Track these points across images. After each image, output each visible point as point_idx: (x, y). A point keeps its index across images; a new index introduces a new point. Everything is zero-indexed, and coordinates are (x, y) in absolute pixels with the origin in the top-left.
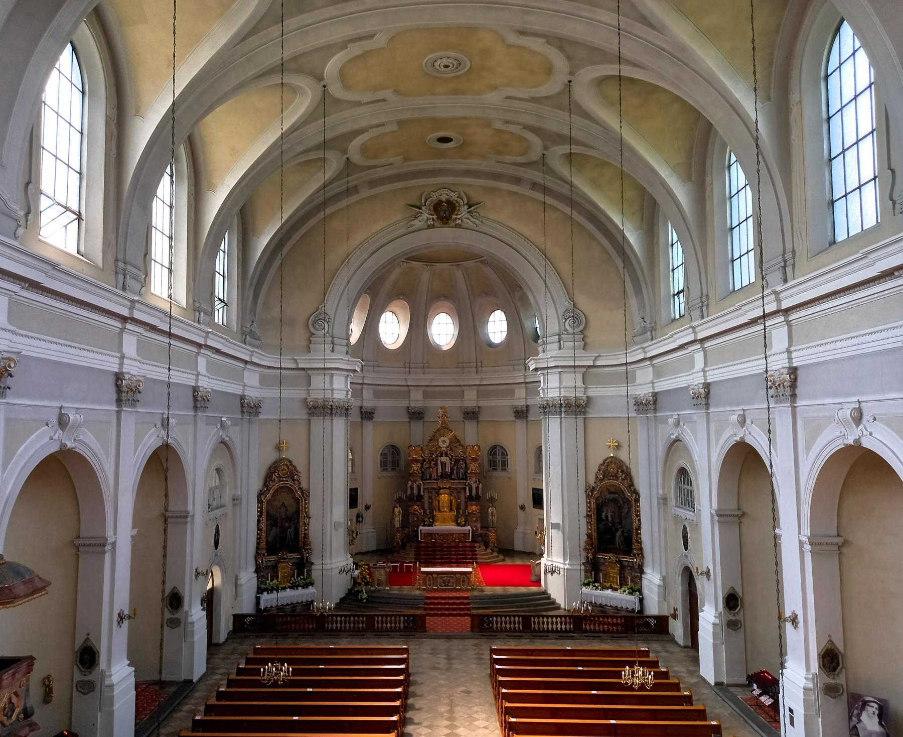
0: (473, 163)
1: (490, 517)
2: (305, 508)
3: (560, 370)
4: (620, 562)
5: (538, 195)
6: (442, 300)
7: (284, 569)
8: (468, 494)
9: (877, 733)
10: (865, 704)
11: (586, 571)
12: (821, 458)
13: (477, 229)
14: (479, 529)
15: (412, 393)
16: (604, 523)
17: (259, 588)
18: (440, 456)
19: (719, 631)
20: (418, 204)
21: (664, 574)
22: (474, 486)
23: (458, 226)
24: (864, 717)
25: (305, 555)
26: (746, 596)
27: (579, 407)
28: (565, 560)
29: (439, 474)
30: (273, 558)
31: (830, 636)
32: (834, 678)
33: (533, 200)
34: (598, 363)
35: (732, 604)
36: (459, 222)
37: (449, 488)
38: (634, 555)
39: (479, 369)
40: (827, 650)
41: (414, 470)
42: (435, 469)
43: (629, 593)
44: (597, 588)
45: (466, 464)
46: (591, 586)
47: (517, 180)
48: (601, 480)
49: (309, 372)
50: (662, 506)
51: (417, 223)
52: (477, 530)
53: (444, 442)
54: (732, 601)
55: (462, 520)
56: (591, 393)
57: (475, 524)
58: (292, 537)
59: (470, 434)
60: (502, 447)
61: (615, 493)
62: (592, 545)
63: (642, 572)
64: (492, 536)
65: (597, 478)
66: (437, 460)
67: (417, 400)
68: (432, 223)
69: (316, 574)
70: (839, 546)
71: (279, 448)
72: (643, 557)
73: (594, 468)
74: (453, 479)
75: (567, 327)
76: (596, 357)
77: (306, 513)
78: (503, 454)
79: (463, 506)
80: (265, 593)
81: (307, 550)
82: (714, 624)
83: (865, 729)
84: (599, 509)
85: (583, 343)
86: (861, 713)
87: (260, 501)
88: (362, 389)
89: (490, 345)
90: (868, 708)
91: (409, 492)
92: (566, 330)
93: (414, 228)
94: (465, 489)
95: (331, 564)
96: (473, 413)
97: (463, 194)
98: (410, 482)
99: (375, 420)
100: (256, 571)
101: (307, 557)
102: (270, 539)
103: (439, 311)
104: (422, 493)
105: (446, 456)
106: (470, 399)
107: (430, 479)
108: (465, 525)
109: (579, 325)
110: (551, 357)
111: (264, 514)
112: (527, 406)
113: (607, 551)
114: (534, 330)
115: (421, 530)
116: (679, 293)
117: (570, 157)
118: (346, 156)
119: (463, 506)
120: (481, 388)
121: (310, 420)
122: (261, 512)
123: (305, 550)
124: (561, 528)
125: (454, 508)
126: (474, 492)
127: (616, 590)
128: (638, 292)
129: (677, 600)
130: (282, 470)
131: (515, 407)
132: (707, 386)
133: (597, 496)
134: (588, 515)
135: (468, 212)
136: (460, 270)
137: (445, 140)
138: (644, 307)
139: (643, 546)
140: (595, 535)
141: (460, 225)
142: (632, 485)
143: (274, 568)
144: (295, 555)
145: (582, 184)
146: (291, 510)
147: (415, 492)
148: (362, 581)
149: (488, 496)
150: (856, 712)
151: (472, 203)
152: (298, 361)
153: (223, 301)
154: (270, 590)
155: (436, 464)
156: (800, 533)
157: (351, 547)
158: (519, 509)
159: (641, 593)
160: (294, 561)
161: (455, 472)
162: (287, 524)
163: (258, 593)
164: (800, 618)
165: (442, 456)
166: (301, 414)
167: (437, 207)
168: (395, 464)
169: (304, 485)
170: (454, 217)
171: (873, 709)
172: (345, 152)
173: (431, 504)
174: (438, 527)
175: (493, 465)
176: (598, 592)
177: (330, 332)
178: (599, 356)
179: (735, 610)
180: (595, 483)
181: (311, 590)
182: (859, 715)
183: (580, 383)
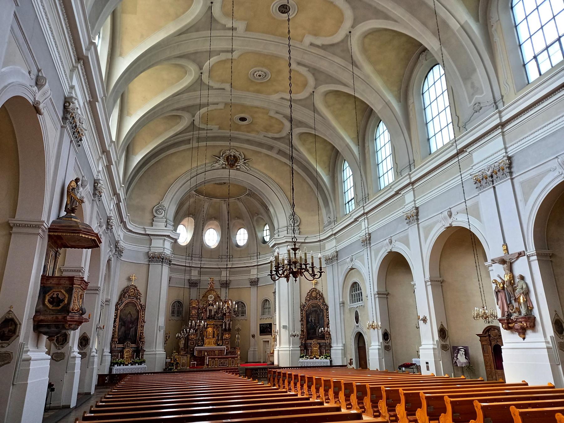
0: (252, 136)
1: (237, 340)
2: (142, 317)
3: (288, 244)
6: (212, 220)
9: (465, 363)
10: (459, 350)
11: (301, 350)
12: (436, 235)
13: (247, 172)
15: (193, 271)
16: (310, 323)
17: (111, 363)
18: (208, 306)
20: (218, 156)
21: (344, 343)
22: (228, 323)
23: (237, 169)
25: (141, 345)
26: (393, 335)
28: (289, 346)
30: (121, 346)
31: (441, 322)
32: (445, 342)
33: (276, 159)
34: (306, 241)
35: (386, 337)
37: (213, 325)
38: (327, 338)
39: (231, 259)
40: (441, 329)
41: (193, 314)
42: (205, 314)
43: (325, 358)
44: (308, 358)
46: (304, 357)
47: (271, 148)
50: (342, 307)
51: (217, 165)
52: (228, 349)
53: (211, 298)
54: (386, 336)
57: (227, 345)
58: (133, 334)
60: (242, 303)
61: (316, 307)
62: (304, 335)
63: (331, 347)
66: (206, 309)
67: (194, 275)
68: (225, 166)
69: (145, 357)
70: (441, 282)
71: (129, 279)
72: (331, 339)
73: (304, 295)
76: (306, 238)
77: (143, 320)
78: (242, 306)
80: (116, 366)
81: (142, 341)
82: (379, 349)
83: (460, 362)
84: (307, 316)
87: (117, 309)
89: (238, 246)
93: (215, 168)
94: (222, 325)
97: (242, 153)
100: (110, 353)
101: (141, 346)
102: (120, 333)
103: (210, 227)
108: (222, 345)
111: (118, 317)
112: (258, 278)
113: (311, 339)
114: (262, 238)
115: (196, 349)
116: (348, 202)
117: (301, 134)
120: (231, 269)
121: (149, 264)
122: (116, 316)
123: (141, 342)
124: (288, 328)
125: (215, 336)
126: (227, 326)
127: (318, 358)
128: (326, 204)
129: (352, 354)
130: (131, 292)
133: (306, 310)
135: (244, 163)
136: (225, 204)
137: (243, 119)
138: (330, 213)
140: (306, 330)
141: (239, 169)
142: (325, 302)
143: (122, 352)
144: (134, 345)
146: (134, 317)
148: (174, 361)
149: (236, 327)
150: (455, 355)
151: (246, 158)
152: (146, 230)
154: (119, 364)
155: (206, 311)
156: (425, 278)
158: (251, 337)
159: (331, 358)
162: (131, 326)
163: (111, 366)
164: (428, 318)
165: (209, 305)
168: (179, 313)
170: (236, 164)
171: (462, 352)
172: (194, 116)
174: (206, 347)
176: (309, 360)
177: (165, 216)
180: (305, 302)
181: (143, 365)
182: (457, 356)
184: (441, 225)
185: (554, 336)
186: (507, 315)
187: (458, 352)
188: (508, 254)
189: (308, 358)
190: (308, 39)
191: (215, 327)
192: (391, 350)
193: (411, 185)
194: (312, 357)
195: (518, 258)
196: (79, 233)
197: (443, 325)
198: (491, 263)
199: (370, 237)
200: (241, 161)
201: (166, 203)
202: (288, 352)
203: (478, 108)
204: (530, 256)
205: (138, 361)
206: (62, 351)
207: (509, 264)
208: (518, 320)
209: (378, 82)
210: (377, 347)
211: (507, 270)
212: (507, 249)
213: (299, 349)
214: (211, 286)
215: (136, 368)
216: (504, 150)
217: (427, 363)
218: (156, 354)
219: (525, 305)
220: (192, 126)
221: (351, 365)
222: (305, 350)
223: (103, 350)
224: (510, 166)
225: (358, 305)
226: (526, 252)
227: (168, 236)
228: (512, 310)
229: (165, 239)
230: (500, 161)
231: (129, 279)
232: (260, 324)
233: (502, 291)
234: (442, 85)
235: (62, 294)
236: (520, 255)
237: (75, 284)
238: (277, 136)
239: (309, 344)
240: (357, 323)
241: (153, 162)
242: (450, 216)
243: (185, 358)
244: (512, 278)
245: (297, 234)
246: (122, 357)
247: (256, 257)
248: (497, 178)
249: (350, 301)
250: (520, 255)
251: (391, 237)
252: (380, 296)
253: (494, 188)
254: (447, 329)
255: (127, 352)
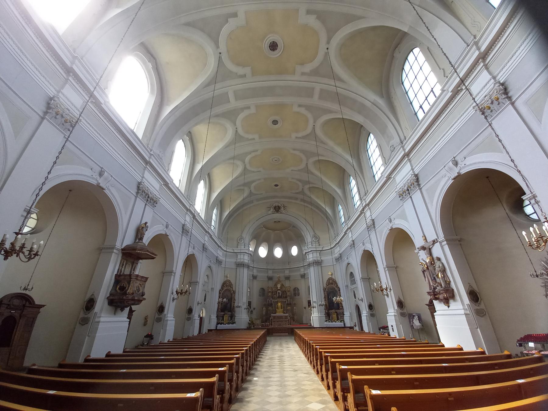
1: (294, 310)
4: (336, 312)
5: (302, 203)
7: (226, 318)
8: (287, 303)
10: (414, 316)
11: (326, 317)
14: (291, 315)
17: (217, 323)
19: (368, 317)
21: (350, 312)
22: (289, 300)
23: (281, 213)
24: (414, 321)
27: (319, 263)
28: (318, 314)
29: (278, 296)
30: (223, 313)
32: (402, 310)
34: (323, 249)
35: (371, 308)
36: (281, 212)
37: (281, 301)
43: (340, 322)
44: (330, 322)
45: (286, 293)
47: (296, 199)
48: (328, 285)
49: (237, 254)
52: (290, 315)
53: (279, 286)
54: (371, 307)
55: (285, 312)
56: (322, 259)
59: (287, 284)
60: (297, 288)
63: (344, 315)
64: (295, 317)
65: (326, 285)
67: (270, 273)
69: (236, 320)
70: (396, 268)
72: (343, 309)
73: (325, 282)
74: (282, 298)
75: (314, 240)
76: (323, 247)
79: (285, 307)
85: (318, 244)
86: (413, 320)
87: (220, 293)
88: (253, 269)
90: (415, 318)
91: (268, 302)
92: (313, 240)
95: (242, 316)
96: (288, 277)
97: (282, 204)
98: (268, 299)
99: (257, 279)
100: (217, 317)
104: (272, 303)
105: (280, 290)
106: (287, 273)
107: (275, 298)
108: (286, 313)
109: (317, 238)
110: (310, 248)
112: (305, 274)
117: (310, 188)
118: (250, 189)
119: (285, 307)
127: (336, 322)
128: (332, 226)
129: (356, 320)
131: (300, 274)
132: (353, 241)
134: (325, 297)
137: (276, 185)
139: (343, 305)
142: (338, 286)
143: (223, 317)
144: (230, 313)
145: (313, 197)
147: (270, 302)
149: (294, 303)
153: (214, 227)
154: (221, 324)
155: (277, 293)
156: (383, 265)
157: (248, 313)
158: (304, 308)
159: (344, 322)
160: (230, 315)
161: (283, 295)
163: (217, 324)
166: (234, 266)
167: (275, 208)
169: (234, 289)
170: (280, 210)
171: (416, 318)
173: (275, 307)
174: (277, 314)
175: (295, 295)
176: (330, 323)
178: (323, 247)
179: (372, 310)
182: (413, 321)
183: (318, 255)
184: (387, 229)
185: (470, 304)
186: (433, 289)
187: (413, 318)
188: (427, 242)
189: (330, 322)
190: (294, 135)
191: (282, 302)
192: (375, 316)
193: (367, 206)
194: (333, 321)
195: (433, 244)
196: (136, 250)
197: (400, 298)
198: (418, 251)
199: (354, 243)
200: (282, 208)
201: (244, 235)
202: (318, 318)
203: (393, 149)
204: (441, 242)
205: (232, 322)
206: (161, 316)
207: (428, 249)
208: (441, 292)
209: (339, 150)
210: (393, 314)
211: (427, 254)
212: (426, 239)
213: (324, 316)
214: (279, 279)
215: (230, 326)
216: (412, 171)
217: (392, 326)
218: (242, 318)
219: (443, 280)
220: (251, 194)
221: (356, 327)
222: (328, 316)
223: (210, 316)
224: (418, 180)
225: (354, 287)
226: (438, 240)
227: (246, 253)
228: (435, 285)
229: (244, 254)
230: (411, 179)
231: (227, 277)
232: (308, 301)
233: (427, 270)
234: (375, 144)
235: (125, 284)
236: (434, 242)
237: (132, 279)
238: (297, 191)
239: (331, 313)
240: (355, 298)
241: (235, 215)
242: (391, 221)
243: (259, 321)
244: (432, 260)
245: (317, 246)
246: (223, 320)
247: (302, 261)
248: (411, 190)
249: (351, 285)
250: (434, 242)
251: (363, 241)
252: (364, 280)
253: (411, 197)
254: (403, 301)
255: (226, 317)
